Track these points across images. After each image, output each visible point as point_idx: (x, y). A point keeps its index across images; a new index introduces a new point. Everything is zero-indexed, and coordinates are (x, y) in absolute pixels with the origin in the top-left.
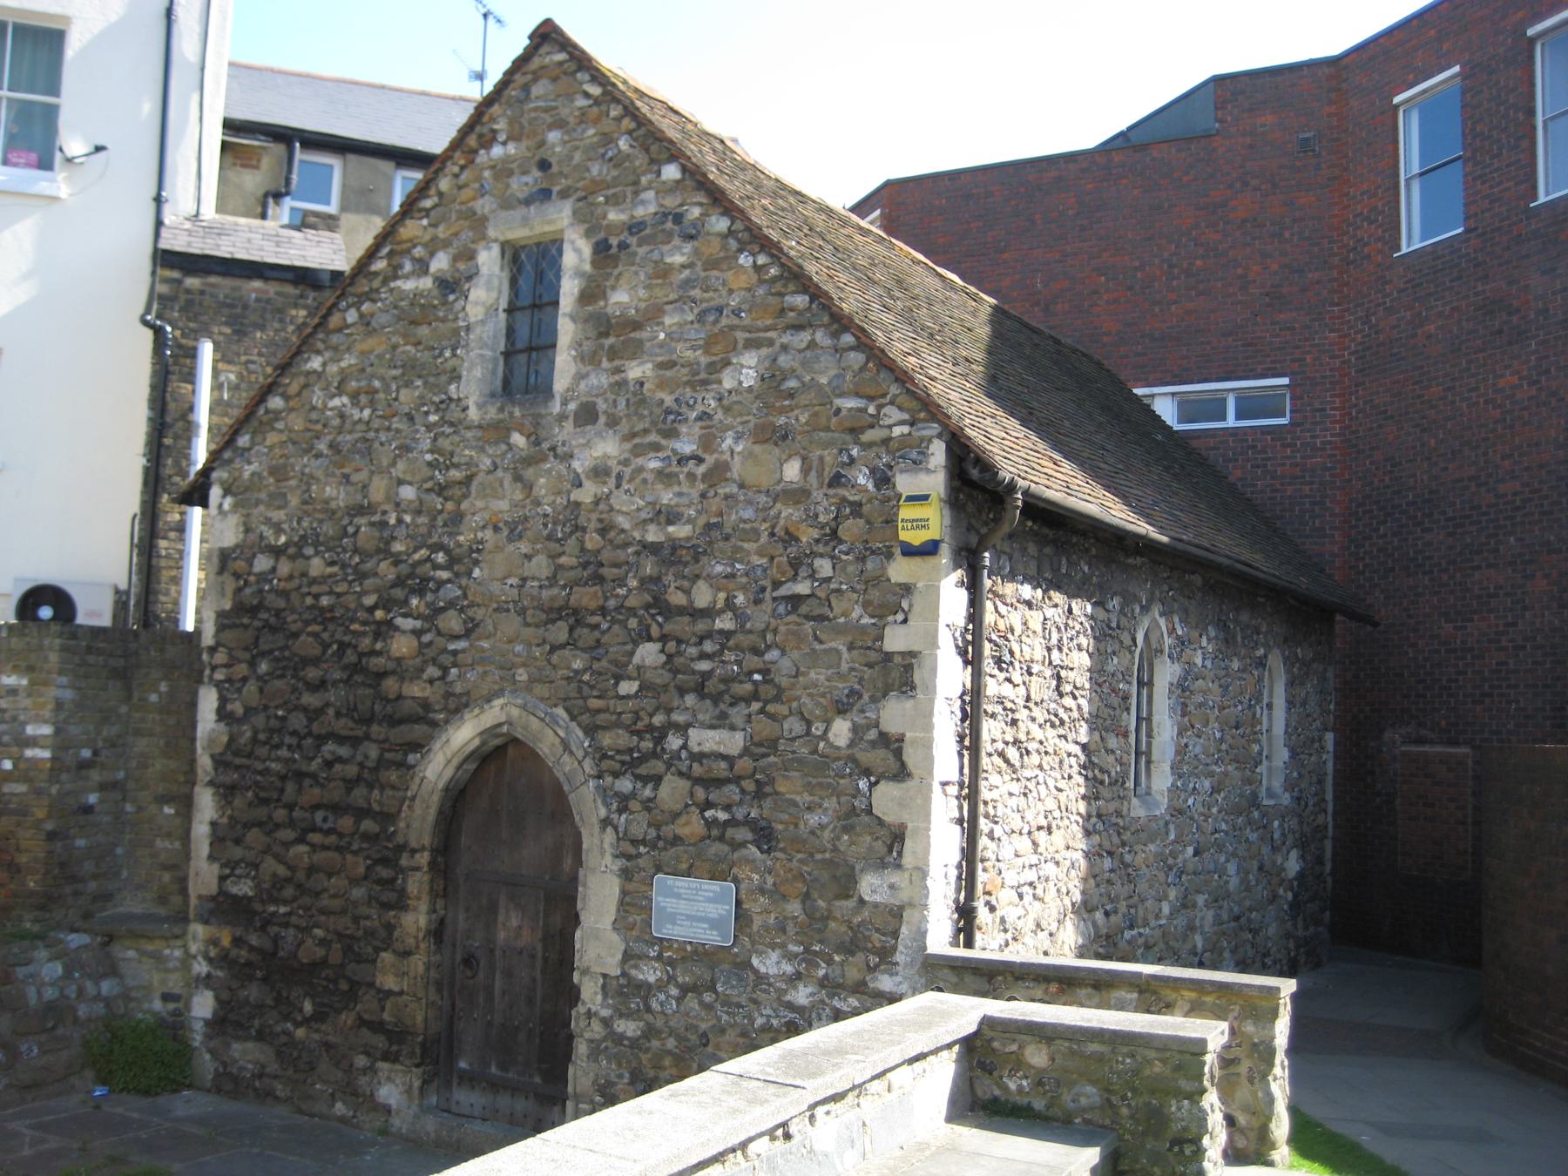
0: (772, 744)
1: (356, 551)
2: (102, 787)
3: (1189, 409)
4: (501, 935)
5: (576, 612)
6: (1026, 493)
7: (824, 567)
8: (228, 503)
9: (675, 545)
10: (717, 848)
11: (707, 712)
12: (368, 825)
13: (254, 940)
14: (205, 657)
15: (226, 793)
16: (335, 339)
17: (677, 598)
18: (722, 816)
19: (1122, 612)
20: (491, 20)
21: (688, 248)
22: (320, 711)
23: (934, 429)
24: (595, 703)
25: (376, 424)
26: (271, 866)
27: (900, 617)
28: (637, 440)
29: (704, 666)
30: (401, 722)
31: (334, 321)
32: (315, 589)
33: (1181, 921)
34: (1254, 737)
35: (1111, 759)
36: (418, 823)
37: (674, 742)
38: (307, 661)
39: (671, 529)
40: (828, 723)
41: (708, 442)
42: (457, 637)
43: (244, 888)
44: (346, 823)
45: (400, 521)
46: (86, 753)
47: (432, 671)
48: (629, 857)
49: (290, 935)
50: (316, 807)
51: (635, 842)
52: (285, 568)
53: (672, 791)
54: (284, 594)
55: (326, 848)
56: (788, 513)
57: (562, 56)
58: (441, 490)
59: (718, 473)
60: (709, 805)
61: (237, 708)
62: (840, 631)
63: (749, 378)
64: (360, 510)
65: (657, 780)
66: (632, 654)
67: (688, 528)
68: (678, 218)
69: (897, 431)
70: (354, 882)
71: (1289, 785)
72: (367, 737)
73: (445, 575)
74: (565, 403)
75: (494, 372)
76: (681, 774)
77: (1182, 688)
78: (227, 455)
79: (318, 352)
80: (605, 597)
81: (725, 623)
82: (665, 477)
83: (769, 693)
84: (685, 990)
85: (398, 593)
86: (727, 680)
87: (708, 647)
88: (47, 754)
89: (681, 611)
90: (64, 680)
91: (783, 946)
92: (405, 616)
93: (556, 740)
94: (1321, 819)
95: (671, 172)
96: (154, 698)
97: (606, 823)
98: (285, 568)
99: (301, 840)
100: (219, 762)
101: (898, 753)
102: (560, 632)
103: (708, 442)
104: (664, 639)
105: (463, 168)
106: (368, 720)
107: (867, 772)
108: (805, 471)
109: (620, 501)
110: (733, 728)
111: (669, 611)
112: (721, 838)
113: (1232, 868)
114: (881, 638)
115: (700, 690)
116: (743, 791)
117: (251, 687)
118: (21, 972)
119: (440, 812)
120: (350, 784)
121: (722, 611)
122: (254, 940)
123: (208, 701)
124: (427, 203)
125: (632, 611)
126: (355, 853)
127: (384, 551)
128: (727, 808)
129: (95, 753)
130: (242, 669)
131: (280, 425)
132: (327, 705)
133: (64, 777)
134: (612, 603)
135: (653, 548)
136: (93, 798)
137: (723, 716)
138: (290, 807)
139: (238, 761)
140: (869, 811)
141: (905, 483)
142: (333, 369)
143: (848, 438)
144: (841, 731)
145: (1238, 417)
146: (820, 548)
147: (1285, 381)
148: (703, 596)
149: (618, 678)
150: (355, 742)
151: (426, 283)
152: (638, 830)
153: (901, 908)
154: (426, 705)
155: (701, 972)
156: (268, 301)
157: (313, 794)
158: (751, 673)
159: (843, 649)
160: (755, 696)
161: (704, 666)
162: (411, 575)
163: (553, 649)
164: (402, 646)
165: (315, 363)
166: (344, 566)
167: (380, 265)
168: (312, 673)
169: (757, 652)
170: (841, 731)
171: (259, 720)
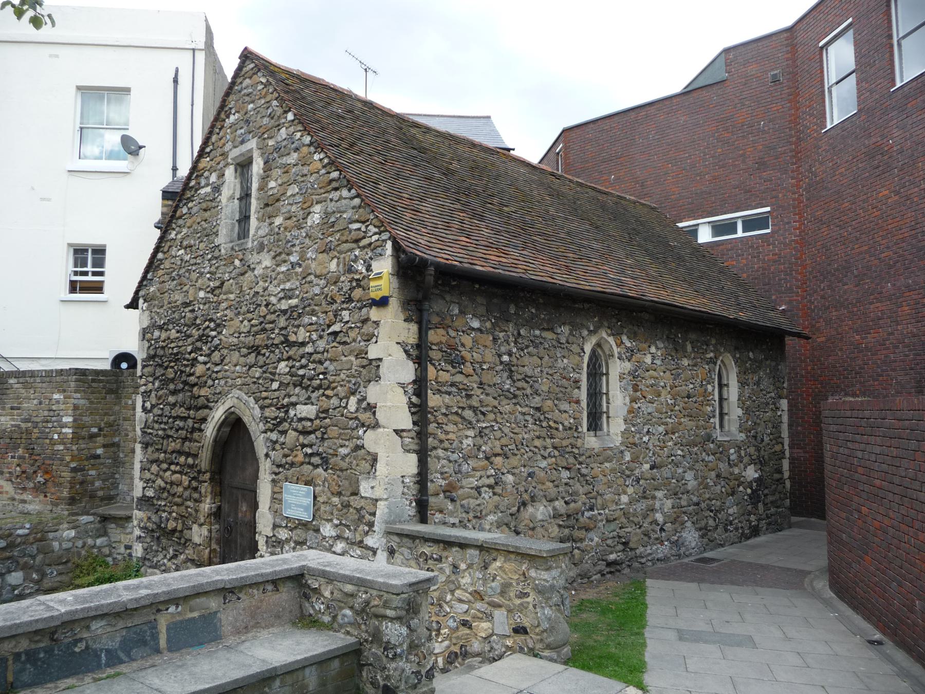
0: (326, 411)
1: (185, 325)
2: (104, 446)
3: (718, 229)
4: (240, 515)
5: (258, 347)
6: (438, 266)
7: (346, 315)
9: (293, 308)
10: (307, 468)
11: (304, 395)
15: (146, 446)
16: (180, 222)
17: (292, 338)
18: (309, 451)
19: (571, 334)
20: (370, 73)
24: (264, 394)
27: (374, 340)
28: (278, 258)
29: (301, 372)
30: (200, 408)
33: (641, 506)
35: (565, 415)
36: (204, 459)
37: (292, 413)
39: (290, 301)
40: (348, 398)
41: (303, 257)
42: (217, 365)
43: (150, 493)
44: (182, 459)
46: (95, 430)
48: (276, 474)
50: (173, 452)
52: (164, 335)
54: (163, 348)
60: (303, 446)
61: (148, 405)
65: (284, 433)
66: (276, 368)
67: (296, 300)
70: (185, 489)
73: (214, 333)
74: (253, 241)
75: (232, 230)
76: (295, 430)
78: (145, 283)
79: (174, 229)
81: (309, 349)
85: (199, 344)
86: (311, 379)
88: (70, 431)
90: (78, 395)
91: (331, 520)
92: (201, 355)
93: (251, 414)
94: (778, 448)
98: (164, 335)
99: (168, 469)
101: (374, 413)
102: (251, 359)
103: (303, 257)
104: (289, 359)
105: (220, 129)
107: (363, 425)
108: (338, 265)
109: (271, 288)
110: (313, 404)
111: (291, 344)
112: (309, 463)
113: (689, 476)
114: (366, 353)
118: (51, 535)
121: (308, 343)
124: (208, 150)
126: (185, 474)
127: (193, 324)
129: (100, 429)
131: (162, 267)
132: (177, 401)
133: (80, 442)
134: (270, 342)
135: (284, 312)
136: (99, 451)
137: (309, 398)
140: (363, 447)
143: (354, 245)
144: (353, 402)
145: (744, 231)
146: (345, 306)
147: (768, 209)
148: (302, 335)
149: (272, 380)
150: (184, 419)
152: (278, 460)
153: (377, 500)
157: (173, 446)
158: (318, 375)
159: (353, 359)
160: (320, 387)
161: (301, 372)
162: (203, 335)
163: (250, 367)
164: (199, 369)
167: (193, 183)
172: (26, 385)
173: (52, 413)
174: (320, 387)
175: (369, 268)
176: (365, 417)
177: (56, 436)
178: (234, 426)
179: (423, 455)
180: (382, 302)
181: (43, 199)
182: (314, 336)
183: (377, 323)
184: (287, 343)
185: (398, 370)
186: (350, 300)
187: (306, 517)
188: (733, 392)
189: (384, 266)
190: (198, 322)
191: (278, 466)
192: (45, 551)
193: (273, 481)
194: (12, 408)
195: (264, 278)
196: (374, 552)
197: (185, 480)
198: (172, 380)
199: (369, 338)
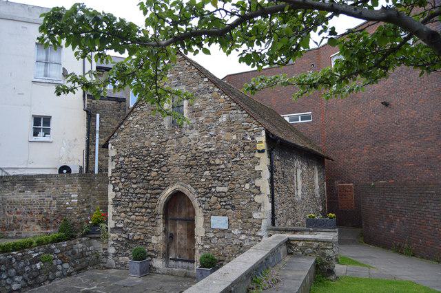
2: (87, 207)
7: (242, 155)
9: (211, 152)
11: (220, 184)
12: (149, 210)
13: (124, 236)
15: (116, 206)
18: (224, 204)
21: (210, 95)
22: (136, 188)
23: (263, 128)
26: (126, 220)
31: (135, 110)
34: (313, 184)
37: (213, 190)
38: (133, 178)
41: (217, 132)
42: (165, 172)
43: (121, 225)
44: (144, 210)
47: (161, 179)
49: (131, 234)
51: (207, 210)
53: (214, 199)
56: (233, 146)
58: (161, 143)
59: (219, 139)
61: (117, 189)
62: (246, 168)
63: (224, 119)
64: (143, 147)
65: (210, 197)
71: (320, 193)
72: (147, 193)
77: (302, 174)
80: (194, 164)
81: (222, 166)
82: (209, 139)
83: (232, 180)
84: (218, 238)
85: (152, 164)
87: (219, 171)
93: (189, 191)
95: (206, 80)
97: (200, 206)
98: (127, 160)
100: (114, 200)
102: (188, 170)
103: (217, 132)
106: (147, 189)
107: (253, 193)
108: (237, 137)
111: (211, 165)
115: (218, 180)
117: (121, 184)
119: (164, 207)
120: (144, 202)
122: (124, 236)
123: (110, 187)
125: (203, 165)
127: (149, 155)
128: (225, 202)
130: (118, 181)
135: (207, 153)
136: (85, 209)
138: (131, 208)
141: (258, 139)
142: (135, 119)
148: (218, 161)
149: (201, 178)
154: (160, 186)
155: (222, 234)
160: (229, 180)
164: (154, 174)
165: (131, 118)
166: (140, 159)
168: (134, 181)
169: (229, 171)
170: (247, 186)
171: (123, 191)
172: (48, 181)
173: (64, 193)
174: (229, 180)
175: (253, 139)
176: (255, 191)
177: (67, 203)
178: (177, 195)
179: (273, 202)
180: (263, 151)
181: (19, 94)
182: (225, 162)
183: (259, 158)
184: (209, 164)
185: (266, 174)
186: (244, 149)
187: (225, 227)
188: (317, 180)
189: (262, 138)
190: (151, 155)
191: (207, 210)
192: (74, 253)
193: (204, 216)
194: (39, 192)
195: (195, 139)
196: (261, 237)
197: (146, 219)
198: (135, 178)
199: (255, 163)
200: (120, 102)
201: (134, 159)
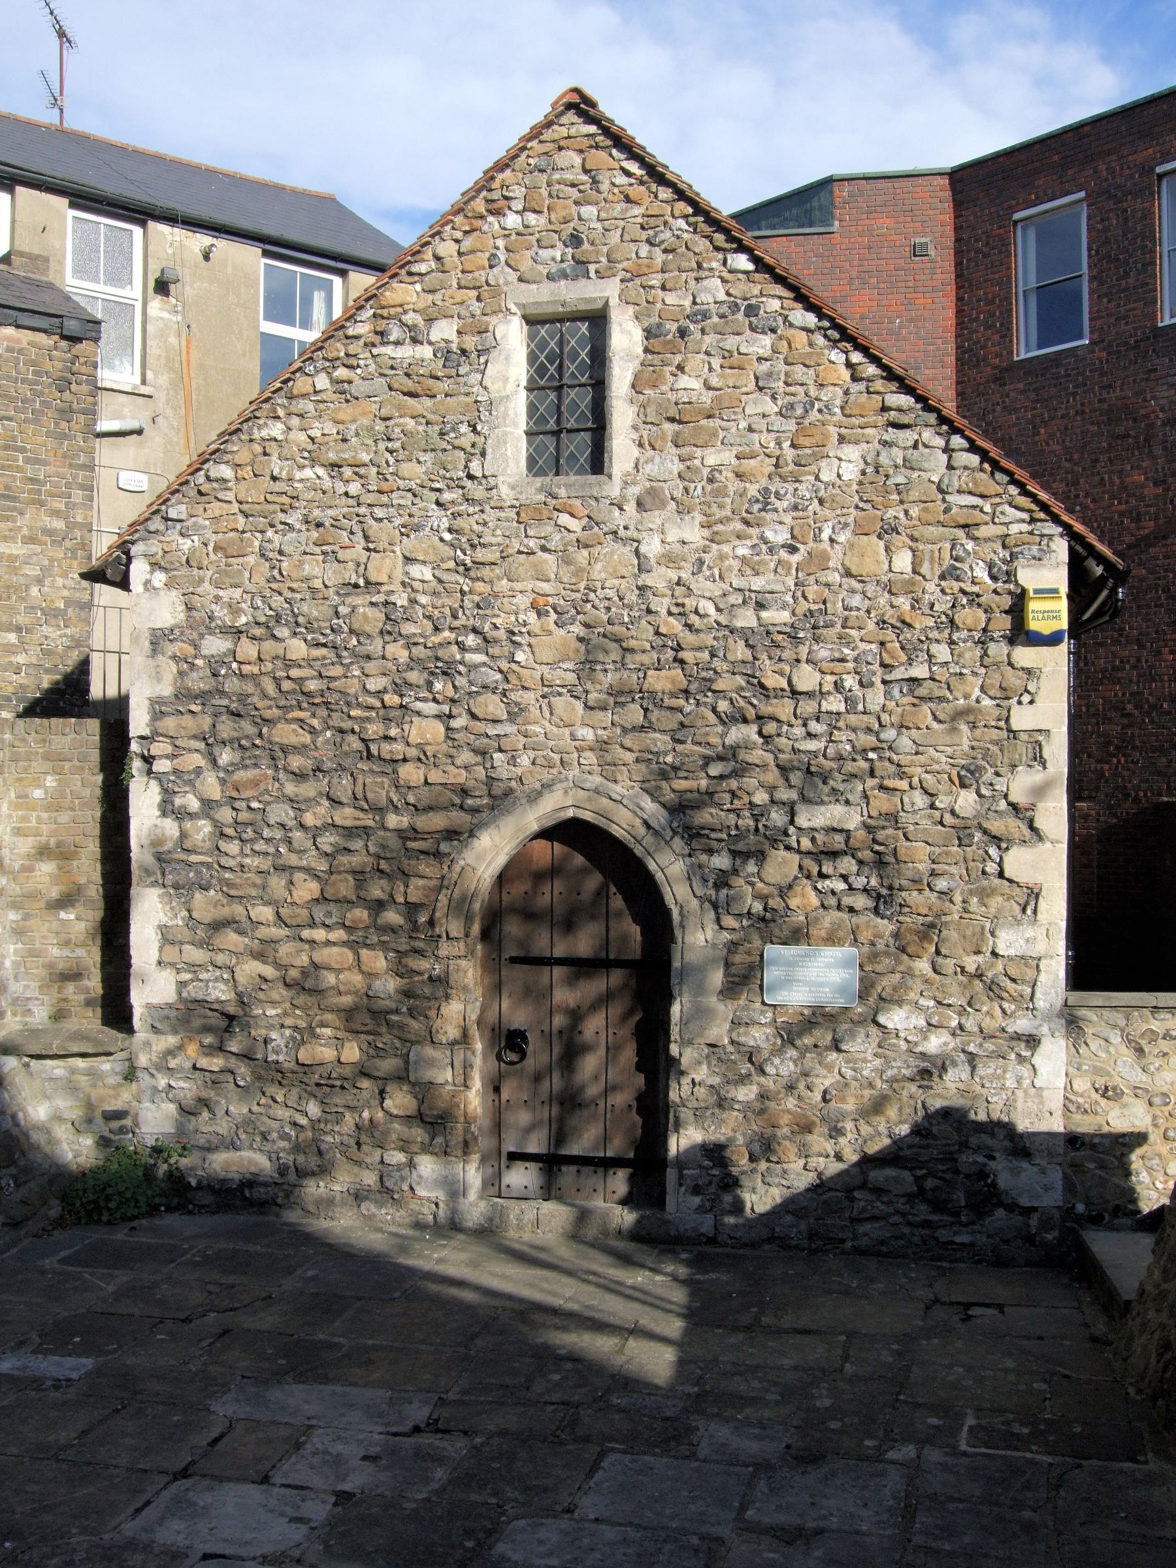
7: (942, 652)
8: (159, 578)
14: (134, 747)
25: (370, 498)
31: (301, 384)
32: (295, 673)
45: (413, 601)
55: (328, 943)
57: (592, 129)
63: (850, 472)
68: (751, 311)
69: (1014, 529)
76: (788, 848)
78: (156, 524)
81: (835, 704)
89: (778, 693)
96: (38, 793)
98: (248, 649)
116: (861, 862)
130: (198, 760)
135: (746, 636)
139: (194, 858)
148: (807, 678)
151: (426, 352)
156: (20, 351)
168: (296, 762)
180: (1053, 640)
182: (850, 682)
198: (300, 749)
200: (74, 340)
201: (298, 649)
